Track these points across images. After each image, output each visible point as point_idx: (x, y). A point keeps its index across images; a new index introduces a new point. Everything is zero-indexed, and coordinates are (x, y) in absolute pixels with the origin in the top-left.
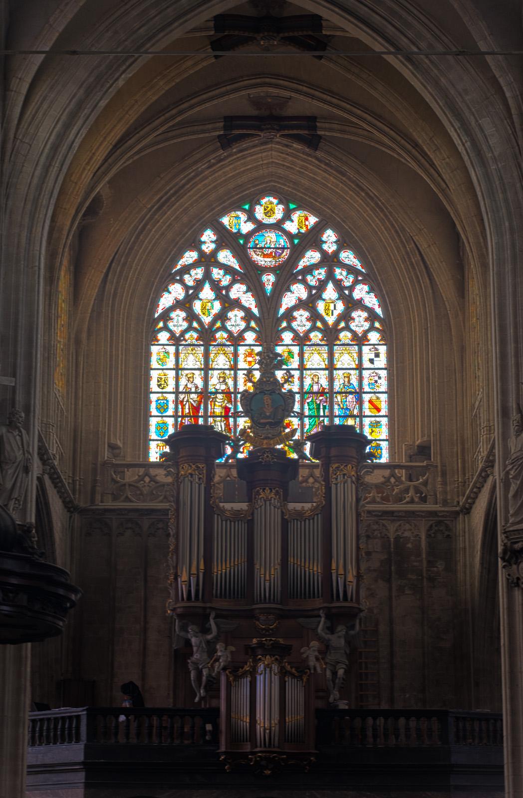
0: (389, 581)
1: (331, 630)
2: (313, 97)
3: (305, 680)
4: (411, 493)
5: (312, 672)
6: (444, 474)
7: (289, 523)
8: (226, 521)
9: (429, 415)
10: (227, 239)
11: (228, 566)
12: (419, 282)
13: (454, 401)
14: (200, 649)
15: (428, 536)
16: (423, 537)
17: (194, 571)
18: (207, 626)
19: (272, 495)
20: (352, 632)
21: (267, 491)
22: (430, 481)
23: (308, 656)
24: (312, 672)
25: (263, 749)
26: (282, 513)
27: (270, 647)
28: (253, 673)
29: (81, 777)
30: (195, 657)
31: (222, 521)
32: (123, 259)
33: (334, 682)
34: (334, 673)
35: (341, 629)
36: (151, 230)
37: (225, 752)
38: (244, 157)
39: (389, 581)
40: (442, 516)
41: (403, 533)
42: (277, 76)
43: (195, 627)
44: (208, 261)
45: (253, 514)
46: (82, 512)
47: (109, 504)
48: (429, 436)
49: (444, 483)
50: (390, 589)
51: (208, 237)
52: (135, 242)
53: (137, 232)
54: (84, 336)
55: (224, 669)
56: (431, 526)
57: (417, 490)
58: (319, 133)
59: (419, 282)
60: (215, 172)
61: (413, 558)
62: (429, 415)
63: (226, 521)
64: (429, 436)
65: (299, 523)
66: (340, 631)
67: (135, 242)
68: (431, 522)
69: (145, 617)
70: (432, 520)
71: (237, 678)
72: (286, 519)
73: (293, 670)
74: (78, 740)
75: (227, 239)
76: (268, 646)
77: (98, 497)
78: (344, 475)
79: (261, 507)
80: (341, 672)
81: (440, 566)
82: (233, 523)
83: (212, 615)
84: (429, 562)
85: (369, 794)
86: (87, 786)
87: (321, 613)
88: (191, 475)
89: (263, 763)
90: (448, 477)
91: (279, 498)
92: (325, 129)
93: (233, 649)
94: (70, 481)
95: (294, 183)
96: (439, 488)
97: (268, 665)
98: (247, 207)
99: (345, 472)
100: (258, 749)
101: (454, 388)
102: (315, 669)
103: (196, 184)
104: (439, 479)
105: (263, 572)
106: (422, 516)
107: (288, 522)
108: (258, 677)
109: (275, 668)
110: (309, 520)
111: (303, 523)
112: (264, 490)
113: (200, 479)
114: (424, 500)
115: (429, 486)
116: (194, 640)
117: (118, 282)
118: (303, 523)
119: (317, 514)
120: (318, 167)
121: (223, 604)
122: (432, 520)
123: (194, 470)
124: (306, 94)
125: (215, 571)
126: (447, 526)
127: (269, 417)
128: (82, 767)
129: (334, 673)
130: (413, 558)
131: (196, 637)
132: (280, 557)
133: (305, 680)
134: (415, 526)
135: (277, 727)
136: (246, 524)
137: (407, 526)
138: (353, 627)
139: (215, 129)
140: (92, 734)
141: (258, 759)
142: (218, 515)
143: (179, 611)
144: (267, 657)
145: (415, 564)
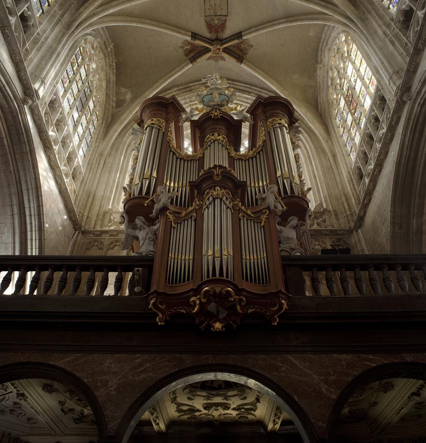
6: (336, 215)
7: (235, 161)
13: (334, 180)
14: (147, 241)
21: (216, 134)
22: (327, 219)
26: (229, 153)
28: (199, 211)
31: (177, 158)
40: (341, 235)
41: (314, 246)
46: (84, 233)
49: (338, 219)
63: (181, 159)
64: (321, 200)
65: (244, 162)
66: (291, 221)
68: (333, 240)
70: (333, 238)
71: (179, 220)
72: (232, 157)
73: (249, 212)
76: (218, 175)
79: (210, 146)
82: (186, 162)
85: (371, 357)
89: (212, 307)
90: (339, 215)
94: (81, 215)
99: (280, 122)
101: (333, 174)
102: (276, 207)
106: (327, 235)
107: (234, 160)
110: (252, 158)
111: (247, 162)
115: (327, 222)
118: (247, 162)
119: (259, 153)
122: (333, 238)
123: (156, 121)
126: (345, 242)
133: (263, 220)
134: (322, 242)
136: (197, 161)
137: (317, 243)
144: (216, 189)
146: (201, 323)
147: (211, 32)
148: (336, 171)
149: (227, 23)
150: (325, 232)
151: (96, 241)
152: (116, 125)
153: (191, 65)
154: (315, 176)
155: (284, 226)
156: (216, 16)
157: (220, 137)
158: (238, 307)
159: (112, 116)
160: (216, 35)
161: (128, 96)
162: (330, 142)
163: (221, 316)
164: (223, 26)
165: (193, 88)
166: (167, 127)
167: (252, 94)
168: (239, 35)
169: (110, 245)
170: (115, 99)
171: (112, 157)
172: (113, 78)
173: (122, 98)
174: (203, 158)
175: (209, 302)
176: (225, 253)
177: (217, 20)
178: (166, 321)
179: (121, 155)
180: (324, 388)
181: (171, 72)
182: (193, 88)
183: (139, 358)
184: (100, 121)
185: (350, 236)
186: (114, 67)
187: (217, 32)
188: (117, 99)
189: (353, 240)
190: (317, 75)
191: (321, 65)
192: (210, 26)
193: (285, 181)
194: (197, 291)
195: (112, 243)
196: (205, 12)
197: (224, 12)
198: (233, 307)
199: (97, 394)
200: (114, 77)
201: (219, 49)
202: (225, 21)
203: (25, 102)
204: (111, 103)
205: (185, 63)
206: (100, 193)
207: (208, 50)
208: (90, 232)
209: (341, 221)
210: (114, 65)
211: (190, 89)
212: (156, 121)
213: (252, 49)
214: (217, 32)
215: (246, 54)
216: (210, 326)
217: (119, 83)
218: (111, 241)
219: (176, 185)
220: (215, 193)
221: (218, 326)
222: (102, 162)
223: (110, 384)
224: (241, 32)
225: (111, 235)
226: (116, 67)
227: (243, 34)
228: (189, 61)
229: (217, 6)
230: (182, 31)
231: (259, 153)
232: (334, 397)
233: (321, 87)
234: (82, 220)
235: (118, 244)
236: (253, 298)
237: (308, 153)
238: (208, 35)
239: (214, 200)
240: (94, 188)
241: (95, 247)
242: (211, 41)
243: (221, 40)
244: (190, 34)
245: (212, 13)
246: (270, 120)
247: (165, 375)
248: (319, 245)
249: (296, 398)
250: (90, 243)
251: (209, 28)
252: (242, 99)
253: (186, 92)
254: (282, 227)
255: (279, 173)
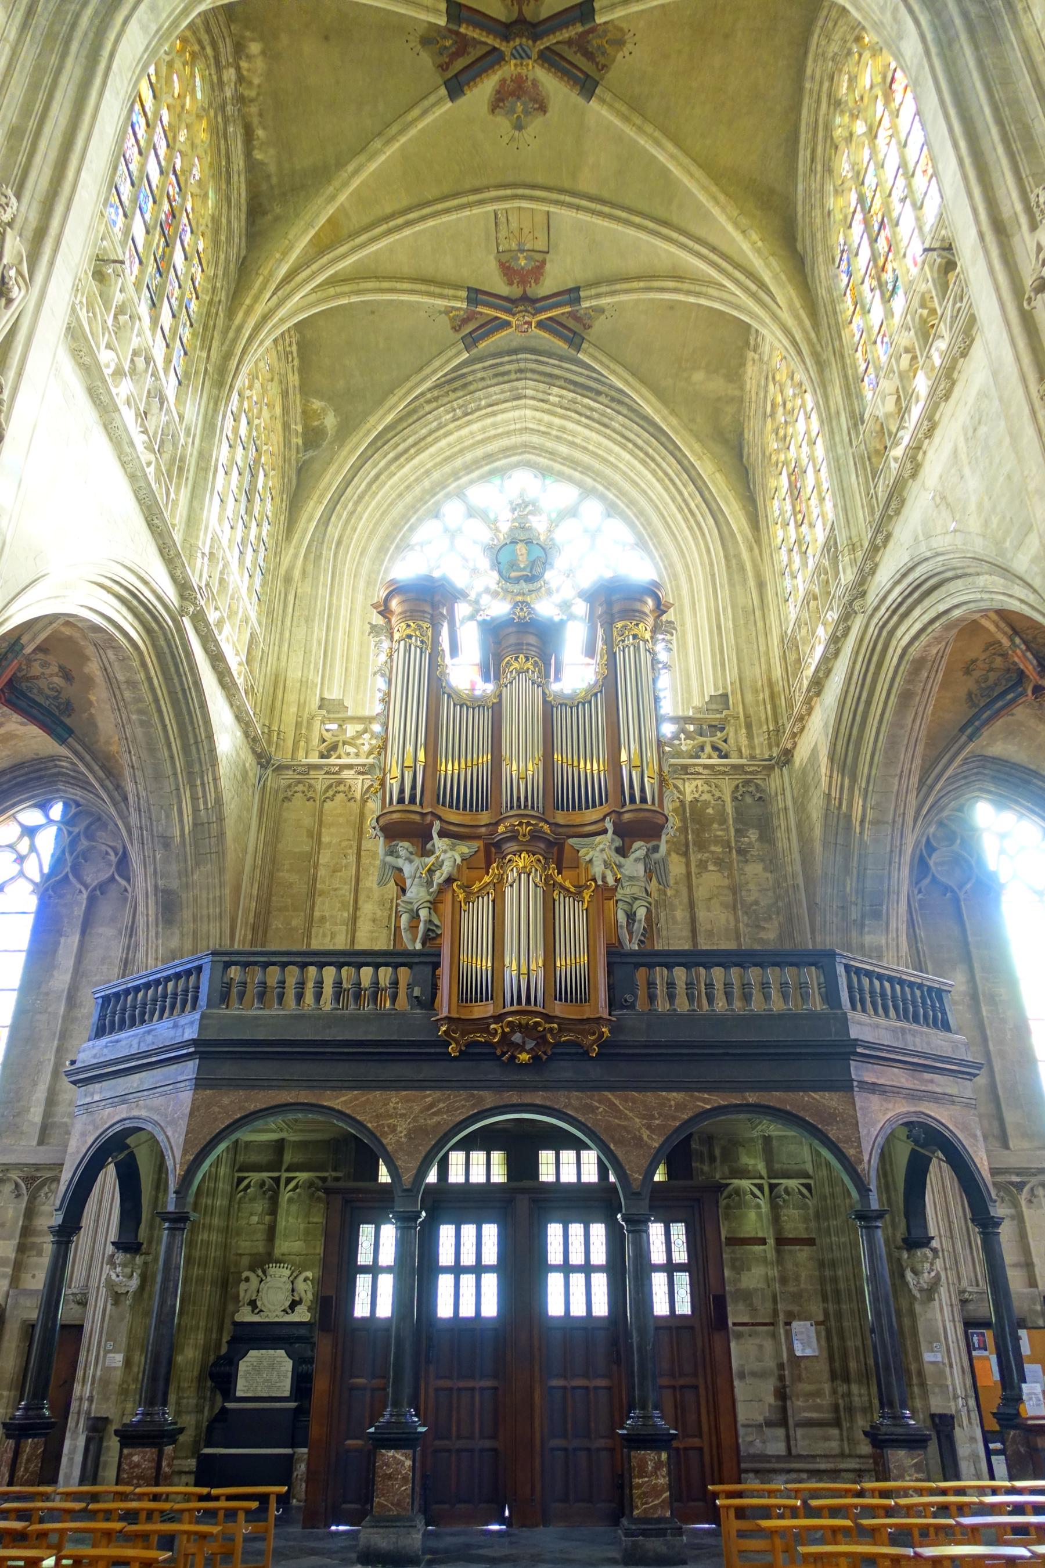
0: (686, 854)
1: (622, 851)
2: (578, 208)
3: (587, 898)
4: (708, 749)
5: (600, 882)
6: (749, 726)
8: (461, 706)
9: (723, 665)
10: (472, 513)
11: (463, 765)
12: (700, 528)
15: (735, 799)
16: (728, 798)
17: (409, 762)
18: (429, 846)
19: (529, 665)
20: (656, 856)
22: (732, 735)
23: (591, 861)
24: (600, 882)
25: (515, 1008)
27: (528, 838)
28: (499, 884)
29: (190, 1068)
30: (408, 894)
31: (455, 705)
32: (350, 504)
33: (631, 933)
34: (631, 917)
35: (639, 848)
36: (384, 483)
37: (447, 1018)
38: (494, 414)
39: (686, 854)
40: (751, 773)
42: (533, 187)
43: (406, 844)
44: (452, 534)
45: (500, 696)
46: (280, 769)
47: (314, 759)
48: (725, 688)
49: (750, 736)
50: (688, 865)
51: (453, 510)
52: (365, 492)
53: (368, 479)
54: (297, 573)
55: (449, 880)
56: (737, 787)
57: (715, 748)
58: (585, 304)
59: (700, 528)
60: (459, 428)
61: (715, 826)
62: (723, 665)
63: (461, 706)
64: (725, 688)
67: (365, 492)
69: (356, 901)
73: (567, 884)
74: (194, 1008)
75: (472, 513)
77: (301, 753)
78: (635, 637)
80: (641, 913)
81: (753, 835)
83: (437, 826)
84: (737, 831)
86: (200, 1083)
87: (609, 825)
88: (410, 637)
89: (517, 1037)
91: (540, 672)
92: (590, 298)
93: (466, 850)
95: (551, 453)
96: (744, 741)
97: (525, 867)
98: (496, 480)
99: (635, 631)
100: (508, 1009)
102: (604, 878)
103: (437, 440)
104: (744, 731)
105: (515, 767)
106: (724, 773)
108: (508, 890)
109: (536, 877)
111: (574, 710)
112: (516, 659)
113: (422, 642)
114: (726, 756)
115: (731, 741)
116: (408, 869)
117: (344, 529)
118: (574, 710)
119: (596, 694)
120: (578, 423)
121: (453, 816)
124: (570, 206)
125: (443, 768)
126: (757, 786)
127: (524, 569)
128: (192, 1050)
129: (631, 917)
130: (715, 826)
131: (411, 861)
132: (541, 753)
133: (587, 898)
135: (541, 973)
138: (656, 849)
139: (455, 298)
140: (224, 996)
141: (507, 1030)
142: (449, 696)
143: (382, 822)
145: (719, 833)
146: (504, 1054)
147: (511, 284)
148: (760, 624)
149: (548, 266)
150: (722, 768)
151: (299, 782)
152: (312, 503)
153: (450, 104)
154: (719, 627)
155: (624, 856)
156: (522, 251)
157: (529, 665)
158: (549, 1036)
159: (299, 471)
160: (521, 289)
161: (330, 421)
162: (756, 551)
163: (528, 1047)
164: (538, 271)
165: (470, 378)
166: (436, 634)
167: (602, 399)
168: (572, 295)
169: (327, 790)
170: (300, 428)
171: (309, 580)
172: (294, 379)
173: (316, 423)
174: (500, 702)
175: (513, 1032)
176: (533, 967)
177: (526, 258)
178: (461, 1052)
179: (326, 570)
180: (645, 1134)
181: (421, 369)
182: (470, 378)
183: (430, 1096)
184: (278, 500)
185: (769, 776)
186: (295, 354)
187: (523, 282)
188: (306, 427)
189: (773, 786)
190: (745, 372)
191: (757, 357)
192: (507, 270)
193: (634, 773)
194: (498, 1018)
195: (330, 786)
196: (498, 245)
197: (540, 245)
198: (544, 1038)
199: (385, 1141)
200: (296, 377)
201: (530, 323)
202: (544, 262)
203: (182, 612)
204: (294, 440)
205: (454, 351)
206: (294, 674)
207: (507, 324)
208: (288, 767)
209: (756, 741)
210: (294, 348)
211: (464, 381)
212: (415, 630)
213: (603, 317)
214: (523, 282)
215: (590, 327)
216: (513, 1057)
217: (306, 389)
218: (328, 783)
219: (456, 767)
220: (521, 865)
221: (524, 1057)
222: (291, 598)
223: (399, 1129)
224: (577, 289)
225: (327, 773)
226: (298, 351)
227: (582, 294)
228: (443, 91)
229: (526, 231)
230: (446, 291)
231: (596, 694)
232: (656, 1145)
233: (753, 406)
234: (269, 742)
235: (341, 788)
236: (565, 1024)
237: (711, 565)
238: (502, 288)
239: (519, 875)
240: (283, 664)
241: (299, 795)
242: (511, 304)
243: (534, 301)
244: (464, 294)
245: (514, 246)
246: (619, 625)
247: (462, 1117)
248: (709, 792)
249: (612, 1146)
250: (289, 786)
251: (505, 275)
252: (579, 408)
253: (454, 390)
254: (622, 859)
255: (624, 757)
